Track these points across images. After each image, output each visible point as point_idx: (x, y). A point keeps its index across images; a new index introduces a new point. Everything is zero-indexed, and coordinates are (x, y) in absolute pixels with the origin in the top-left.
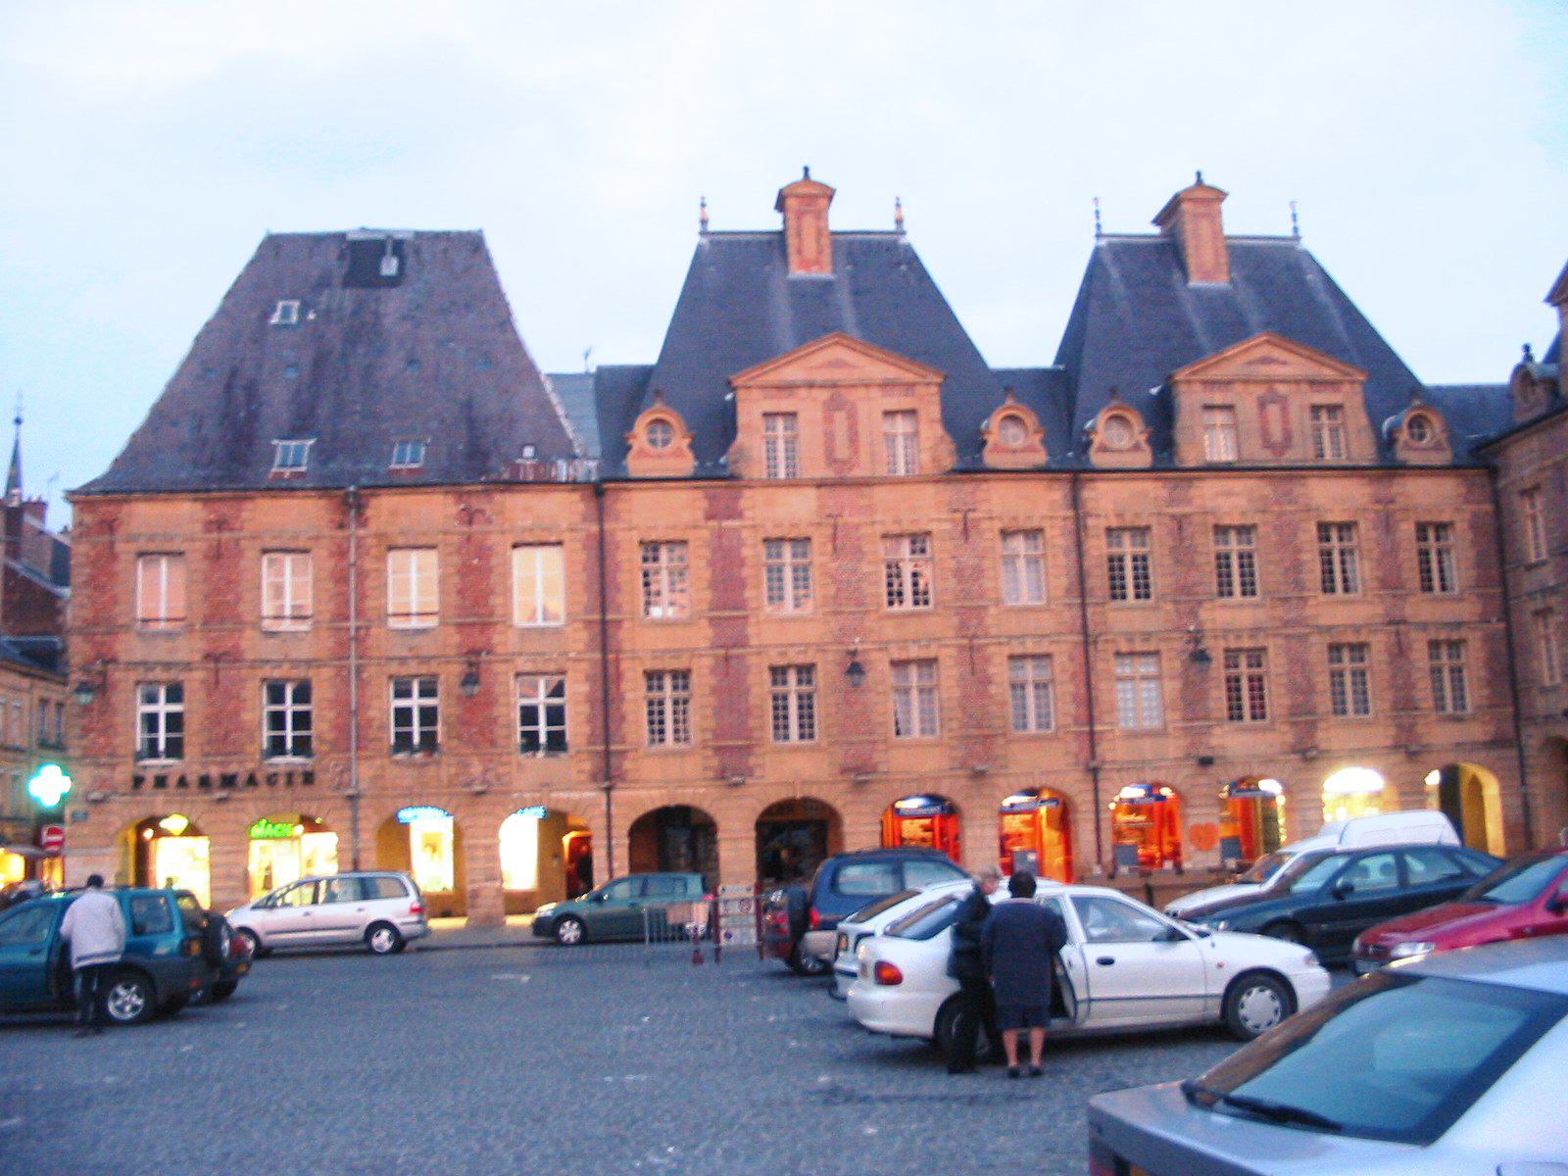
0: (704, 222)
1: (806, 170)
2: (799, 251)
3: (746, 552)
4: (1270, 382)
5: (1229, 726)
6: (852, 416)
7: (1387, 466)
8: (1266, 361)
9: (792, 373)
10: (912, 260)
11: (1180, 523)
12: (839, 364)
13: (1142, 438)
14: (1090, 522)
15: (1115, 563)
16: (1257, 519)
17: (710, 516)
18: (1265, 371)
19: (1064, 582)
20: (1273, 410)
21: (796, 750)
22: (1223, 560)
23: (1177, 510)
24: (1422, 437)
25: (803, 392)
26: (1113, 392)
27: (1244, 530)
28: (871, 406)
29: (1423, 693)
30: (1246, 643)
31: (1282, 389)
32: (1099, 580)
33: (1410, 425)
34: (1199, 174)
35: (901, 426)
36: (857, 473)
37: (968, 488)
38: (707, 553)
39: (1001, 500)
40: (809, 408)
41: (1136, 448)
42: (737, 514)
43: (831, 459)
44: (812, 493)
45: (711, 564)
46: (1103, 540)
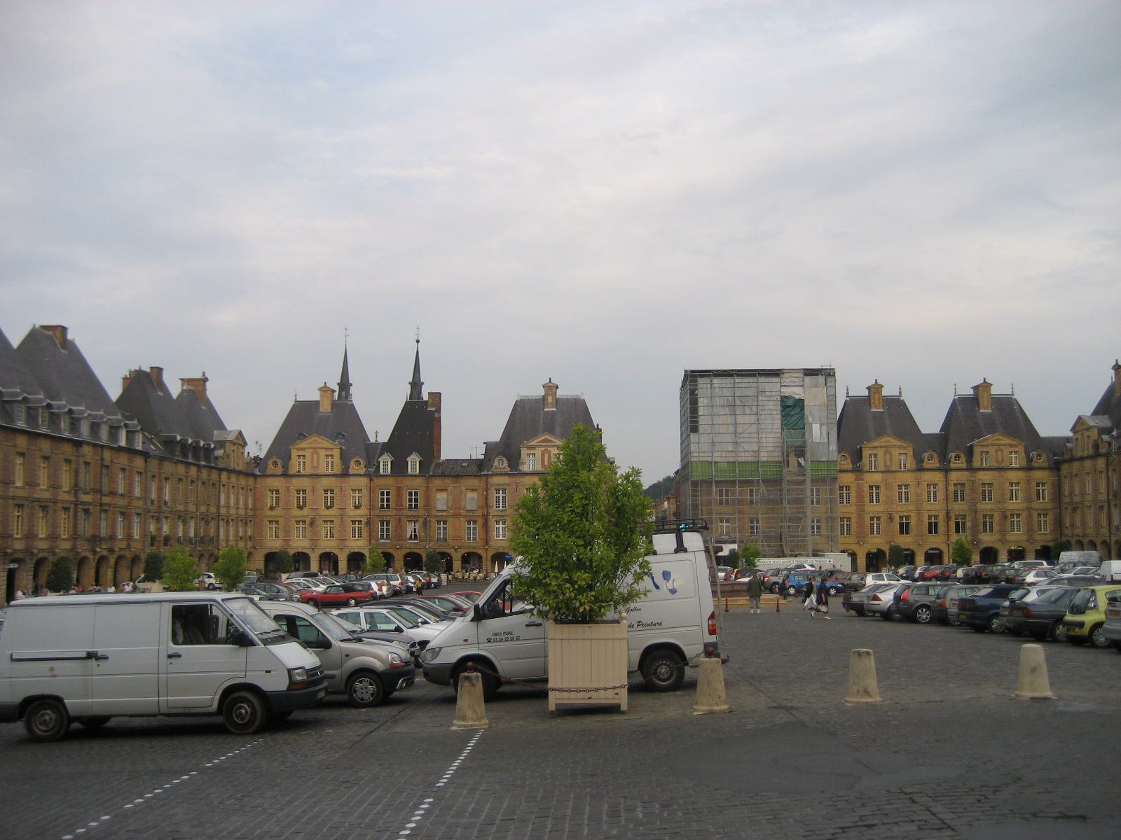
0: (848, 393)
1: (876, 380)
2: (874, 403)
3: (865, 489)
4: (999, 445)
5: (983, 534)
6: (891, 454)
7: (1029, 468)
8: (997, 439)
9: (876, 444)
10: (903, 404)
11: (973, 482)
12: (888, 441)
13: (964, 460)
14: (950, 482)
15: (956, 493)
16: (993, 481)
17: (856, 480)
18: (998, 442)
19: (943, 497)
20: (999, 453)
21: (876, 537)
22: (984, 492)
23: (972, 479)
24: (1040, 459)
25: (879, 449)
26: (957, 448)
27: (990, 484)
28: (895, 452)
29: (1036, 527)
30: (989, 513)
31: (1002, 447)
32: (951, 496)
33: (1037, 456)
34: (985, 379)
35: (902, 457)
36: (891, 469)
37: (919, 473)
38: (855, 489)
39: (928, 477)
40: (880, 453)
41: (963, 463)
42: (863, 479)
43: (885, 465)
44: (881, 474)
45: (856, 491)
46: (953, 487)
